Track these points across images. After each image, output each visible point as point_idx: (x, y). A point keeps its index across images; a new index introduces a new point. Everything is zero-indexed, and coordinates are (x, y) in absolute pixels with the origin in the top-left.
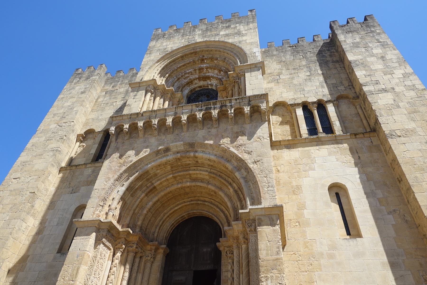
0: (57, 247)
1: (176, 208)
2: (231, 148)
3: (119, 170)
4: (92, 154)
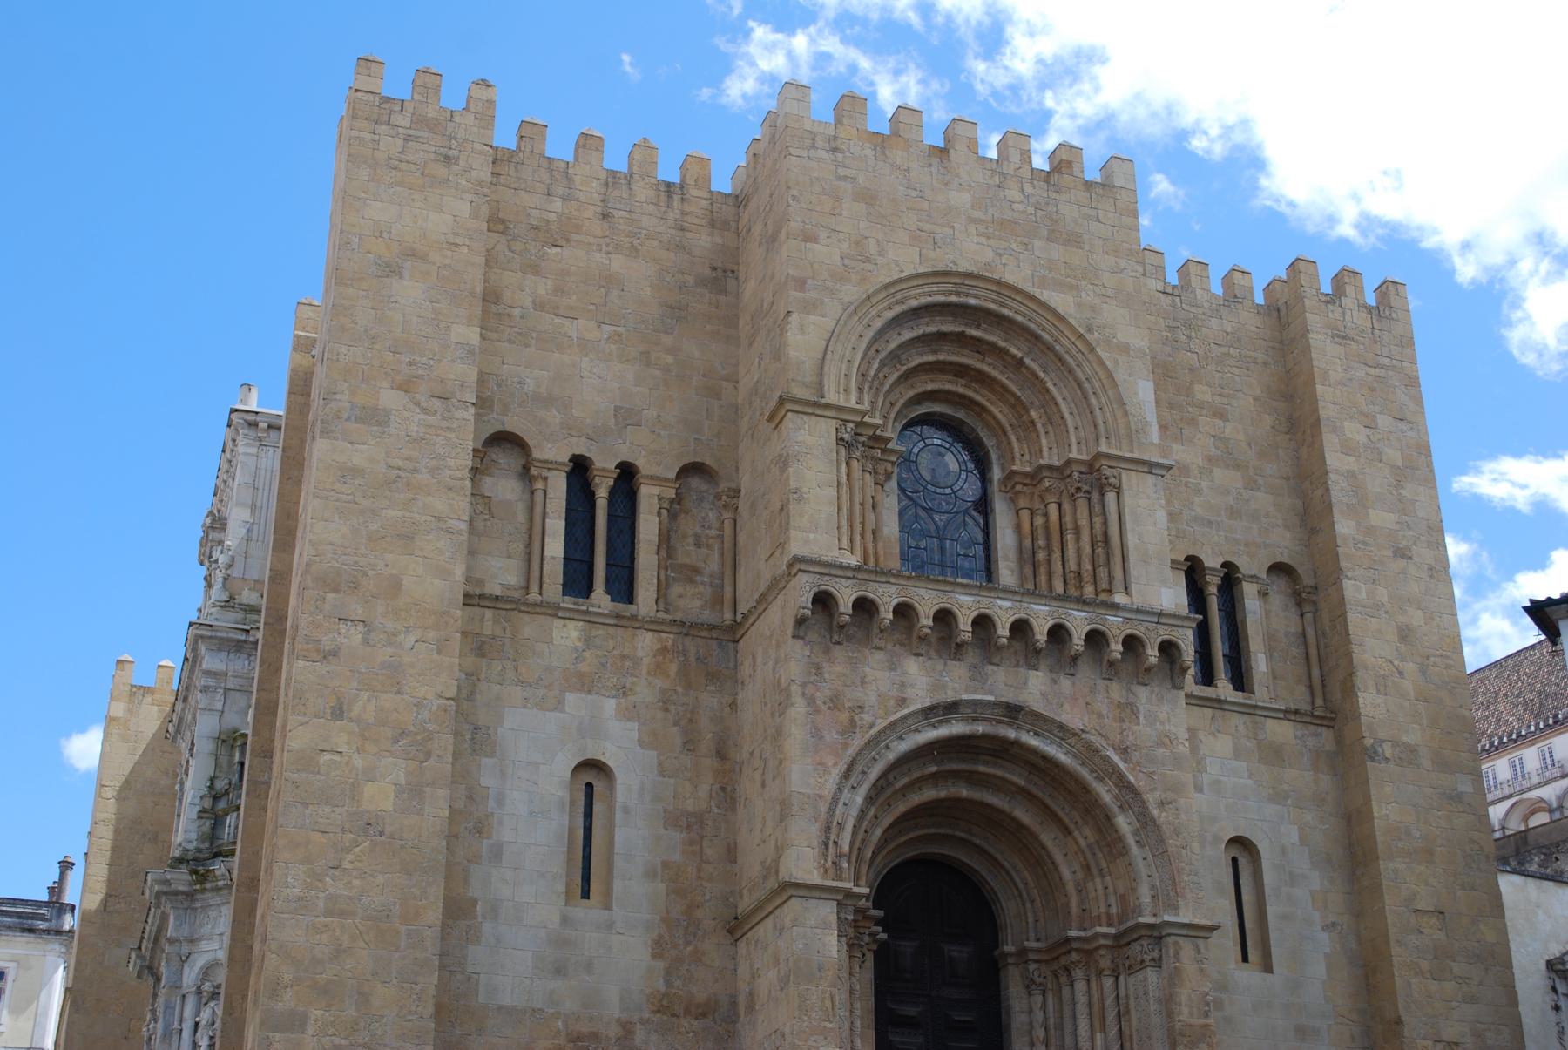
0: (561, 888)
1: (903, 839)
2: (1111, 749)
3: (846, 746)
4: (553, 558)
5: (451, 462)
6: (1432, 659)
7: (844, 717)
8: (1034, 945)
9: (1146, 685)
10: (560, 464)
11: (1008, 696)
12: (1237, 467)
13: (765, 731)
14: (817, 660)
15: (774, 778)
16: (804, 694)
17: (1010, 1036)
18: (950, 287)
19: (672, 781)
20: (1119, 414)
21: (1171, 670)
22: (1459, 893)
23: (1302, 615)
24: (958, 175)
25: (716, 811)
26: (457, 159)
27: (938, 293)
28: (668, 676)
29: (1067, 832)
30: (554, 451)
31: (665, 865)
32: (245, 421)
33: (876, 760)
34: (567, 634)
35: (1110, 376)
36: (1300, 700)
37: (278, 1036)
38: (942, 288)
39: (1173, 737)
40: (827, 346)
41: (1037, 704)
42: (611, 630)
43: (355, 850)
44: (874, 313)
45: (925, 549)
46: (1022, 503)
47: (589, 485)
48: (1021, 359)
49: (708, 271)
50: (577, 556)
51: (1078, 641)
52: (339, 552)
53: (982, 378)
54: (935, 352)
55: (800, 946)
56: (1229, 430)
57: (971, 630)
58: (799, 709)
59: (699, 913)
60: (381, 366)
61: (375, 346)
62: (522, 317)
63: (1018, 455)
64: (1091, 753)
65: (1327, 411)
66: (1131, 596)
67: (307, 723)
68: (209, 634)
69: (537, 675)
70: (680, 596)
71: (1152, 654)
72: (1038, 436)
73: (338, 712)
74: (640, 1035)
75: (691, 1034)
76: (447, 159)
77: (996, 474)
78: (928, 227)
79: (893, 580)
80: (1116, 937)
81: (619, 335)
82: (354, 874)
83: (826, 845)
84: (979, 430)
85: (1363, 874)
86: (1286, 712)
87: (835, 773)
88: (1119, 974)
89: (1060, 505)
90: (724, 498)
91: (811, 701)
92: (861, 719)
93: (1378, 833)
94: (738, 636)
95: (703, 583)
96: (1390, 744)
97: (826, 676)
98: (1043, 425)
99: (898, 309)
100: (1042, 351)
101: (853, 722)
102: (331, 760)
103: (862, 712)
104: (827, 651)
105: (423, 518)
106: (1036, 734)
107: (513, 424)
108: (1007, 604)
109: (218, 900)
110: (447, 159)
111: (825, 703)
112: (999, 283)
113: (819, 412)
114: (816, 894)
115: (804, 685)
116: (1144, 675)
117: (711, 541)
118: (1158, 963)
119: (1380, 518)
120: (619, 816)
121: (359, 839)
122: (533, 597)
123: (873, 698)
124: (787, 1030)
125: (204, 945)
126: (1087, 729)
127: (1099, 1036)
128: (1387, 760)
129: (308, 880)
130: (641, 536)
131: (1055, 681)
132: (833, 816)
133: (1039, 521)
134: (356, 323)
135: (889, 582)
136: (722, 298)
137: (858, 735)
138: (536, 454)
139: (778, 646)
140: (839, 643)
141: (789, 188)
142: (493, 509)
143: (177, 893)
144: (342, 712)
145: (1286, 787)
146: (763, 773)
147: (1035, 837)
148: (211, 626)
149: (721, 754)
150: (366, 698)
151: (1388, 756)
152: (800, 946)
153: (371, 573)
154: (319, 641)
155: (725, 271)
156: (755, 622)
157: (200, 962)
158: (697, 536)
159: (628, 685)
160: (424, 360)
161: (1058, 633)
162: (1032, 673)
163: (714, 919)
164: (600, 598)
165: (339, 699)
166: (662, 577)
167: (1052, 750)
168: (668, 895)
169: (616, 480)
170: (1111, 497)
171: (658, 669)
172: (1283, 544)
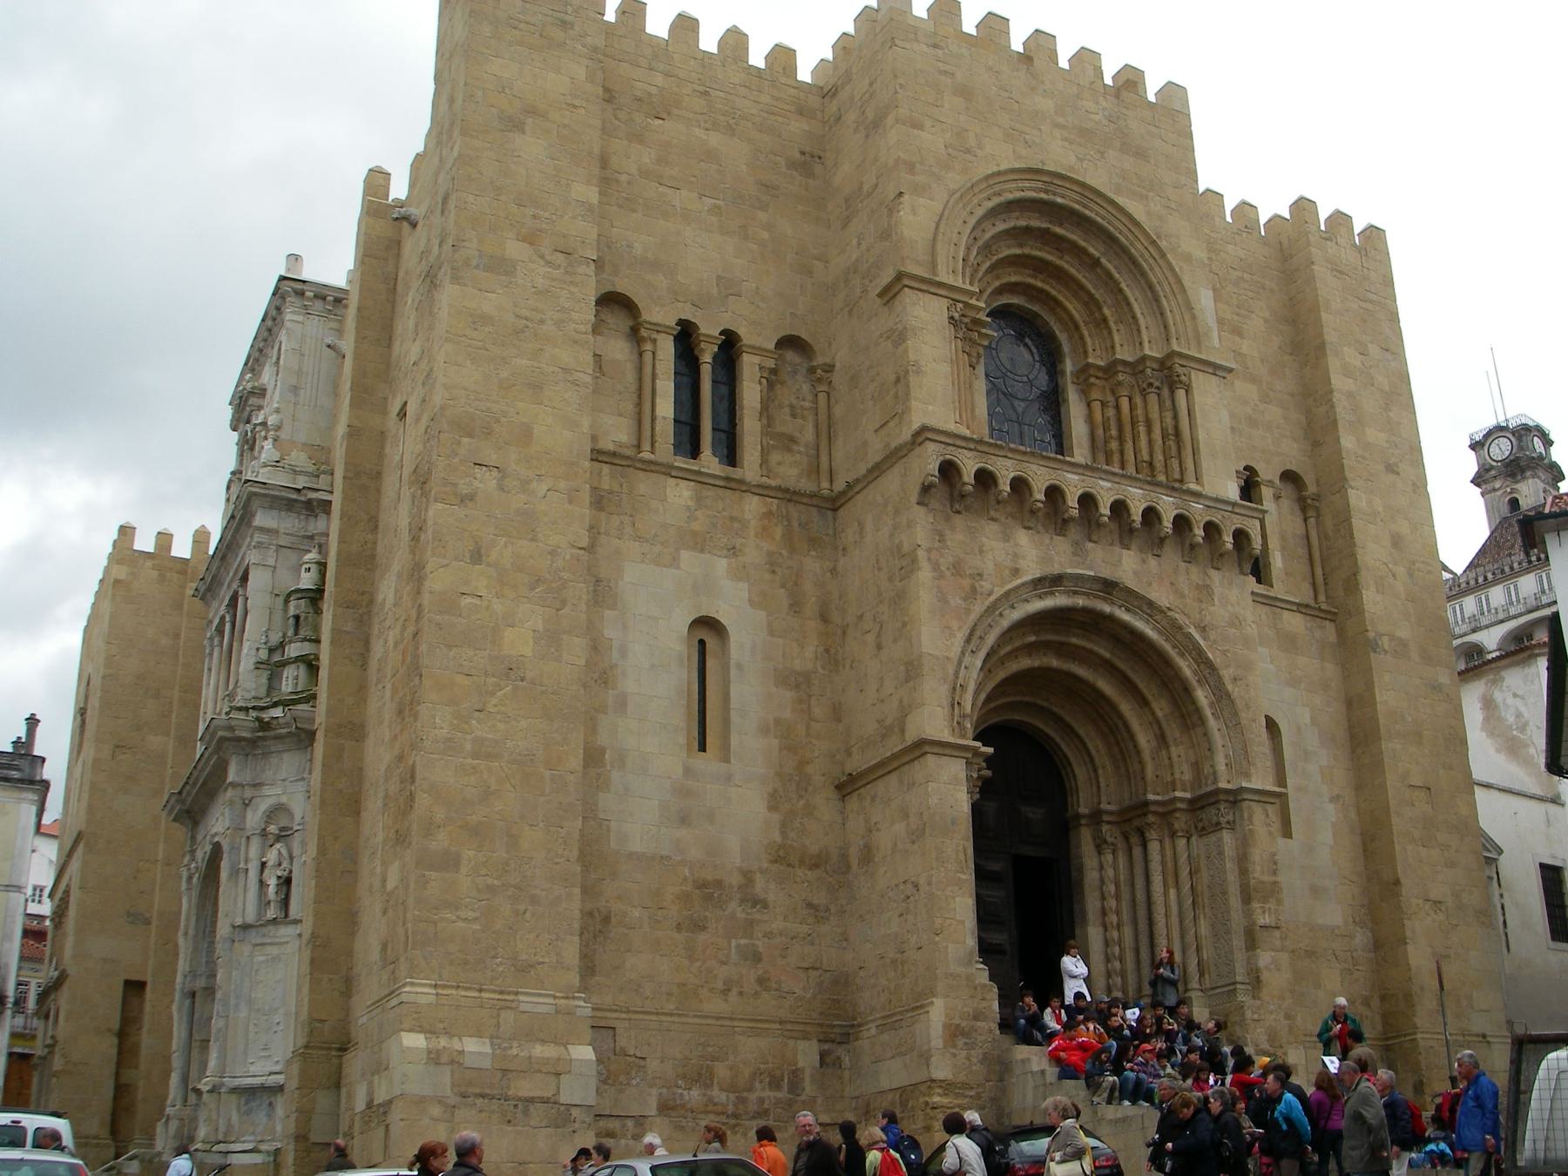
0: (682, 740)
3: (968, 611)
4: (664, 418)
5: (575, 316)
6: (1417, 565)
7: (966, 582)
8: (1109, 807)
9: (1218, 569)
10: (668, 327)
11: (1105, 573)
12: (1253, 379)
13: (880, 594)
14: (940, 528)
15: (895, 641)
16: (929, 559)
17: (1082, 893)
18: (1040, 185)
19: (780, 641)
20: (1187, 317)
21: (1239, 558)
22: (1441, 772)
23: (1305, 520)
24: (1042, 82)
25: (821, 671)
26: (572, 25)
27: (1030, 189)
28: (774, 539)
29: (1143, 702)
30: (662, 314)
31: (777, 722)
32: (292, 288)
33: (991, 626)
34: (680, 494)
35: (1179, 281)
36: (1304, 594)
37: (433, 874)
38: (1033, 184)
39: (1241, 618)
40: (937, 228)
41: (1131, 583)
42: (721, 491)
43: (498, 694)
44: (976, 201)
45: (1007, 432)
46: (1095, 395)
47: (692, 350)
48: (1098, 260)
49: (797, 155)
50: (683, 419)
51: (1167, 524)
52: (472, 397)
53: (1059, 275)
54: (1021, 246)
55: (936, 801)
56: (1245, 346)
57: (1077, 506)
58: (925, 574)
59: (809, 769)
60: (507, 218)
61: (501, 198)
62: (629, 183)
63: (1090, 350)
64: (1174, 629)
65: (1330, 336)
66: (1203, 486)
67: (447, 565)
68: (262, 491)
69: (654, 531)
70: (779, 464)
71: (1228, 539)
72: (1110, 333)
73: (477, 557)
74: (760, 884)
75: (806, 884)
76: (565, 25)
77: (1069, 366)
78: (1018, 126)
79: (1010, 455)
80: (1191, 801)
81: (719, 208)
82: (499, 717)
83: (953, 705)
84: (1052, 324)
85: (1363, 753)
86: (1298, 605)
87: (960, 637)
88: (1191, 835)
89: (1130, 399)
90: (819, 371)
91: (936, 567)
92: (982, 587)
93: (1380, 717)
94: (839, 504)
95: (799, 452)
96: (1387, 637)
97: (949, 543)
98: (1115, 323)
99: (996, 200)
100: (1116, 253)
101: (974, 590)
102: (471, 603)
103: (981, 580)
104: (948, 519)
105: (551, 369)
106: (1128, 610)
107: (623, 286)
108: (1108, 485)
109: (280, 747)
110: (565, 25)
111: (948, 569)
112: (1083, 185)
113: (933, 290)
114: (948, 751)
115: (929, 550)
116: (1217, 558)
117: (805, 412)
118: (1232, 825)
119: (1375, 435)
120: (733, 672)
121: (502, 683)
122: (646, 455)
123: (990, 565)
124: (922, 881)
125: (267, 791)
126: (1173, 608)
127: (1172, 892)
128: (1386, 652)
129: (455, 722)
130: (745, 402)
131: (1144, 561)
132: (957, 678)
133: (1111, 412)
134: (482, 174)
135: (1005, 457)
136: (810, 181)
137: (979, 601)
138: (645, 316)
139: (897, 511)
140: (959, 512)
141: (895, 76)
142: (604, 367)
143: (239, 739)
144: (481, 556)
145: (1299, 672)
146: (879, 635)
147: (1114, 707)
148: (265, 484)
149: (824, 618)
150: (502, 543)
151: (1386, 648)
152: (936, 801)
153: (503, 420)
154: (456, 484)
155: (813, 156)
156: (861, 490)
157: (263, 806)
158: (792, 407)
159: (738, 546)
160: (547, 215)
161: (1151, 515)
162: (1125, 552)
163: (823, 775)
164: (709, 461)
165: (477, 543)
166: (765, 443)
167: (1140, 625)
168: (780, 750)
169: (720, 347)
170: (1181, 394)
171: (764, 532)
172: (1292, 454)
